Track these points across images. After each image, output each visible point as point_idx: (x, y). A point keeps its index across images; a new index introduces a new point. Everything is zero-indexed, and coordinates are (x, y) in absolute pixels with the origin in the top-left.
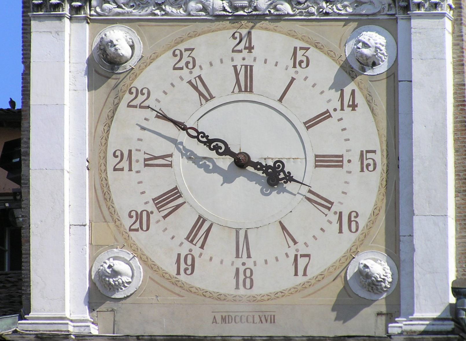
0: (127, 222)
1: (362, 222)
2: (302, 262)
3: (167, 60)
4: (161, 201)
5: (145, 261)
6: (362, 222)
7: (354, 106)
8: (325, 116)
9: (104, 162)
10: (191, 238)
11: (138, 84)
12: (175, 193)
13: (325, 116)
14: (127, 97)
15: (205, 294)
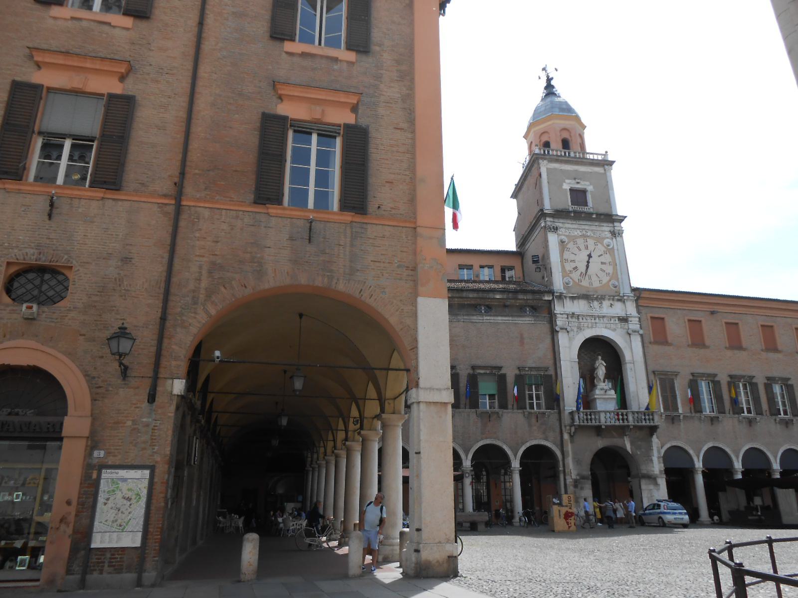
0: (568, 272)
1: (611, 274)
2: (601, 282)
3: (572, 243)
4: (574, 269)
5: (572, 280)
6: (611, 274)
7: (607, 254)
8: (602, 255)
9: (563, 261)
10: (580, 276)
11: (567, 247)
12: (576, 267)
13: (602, 255)
14: (566, 249)
15: (583, 286)
